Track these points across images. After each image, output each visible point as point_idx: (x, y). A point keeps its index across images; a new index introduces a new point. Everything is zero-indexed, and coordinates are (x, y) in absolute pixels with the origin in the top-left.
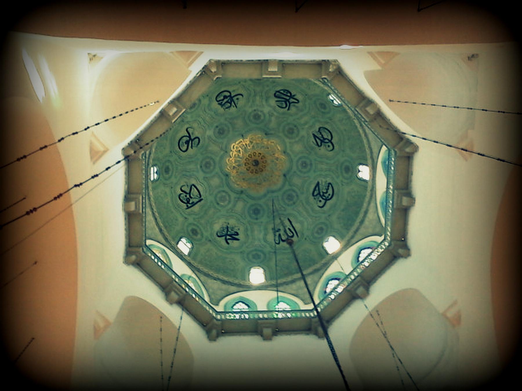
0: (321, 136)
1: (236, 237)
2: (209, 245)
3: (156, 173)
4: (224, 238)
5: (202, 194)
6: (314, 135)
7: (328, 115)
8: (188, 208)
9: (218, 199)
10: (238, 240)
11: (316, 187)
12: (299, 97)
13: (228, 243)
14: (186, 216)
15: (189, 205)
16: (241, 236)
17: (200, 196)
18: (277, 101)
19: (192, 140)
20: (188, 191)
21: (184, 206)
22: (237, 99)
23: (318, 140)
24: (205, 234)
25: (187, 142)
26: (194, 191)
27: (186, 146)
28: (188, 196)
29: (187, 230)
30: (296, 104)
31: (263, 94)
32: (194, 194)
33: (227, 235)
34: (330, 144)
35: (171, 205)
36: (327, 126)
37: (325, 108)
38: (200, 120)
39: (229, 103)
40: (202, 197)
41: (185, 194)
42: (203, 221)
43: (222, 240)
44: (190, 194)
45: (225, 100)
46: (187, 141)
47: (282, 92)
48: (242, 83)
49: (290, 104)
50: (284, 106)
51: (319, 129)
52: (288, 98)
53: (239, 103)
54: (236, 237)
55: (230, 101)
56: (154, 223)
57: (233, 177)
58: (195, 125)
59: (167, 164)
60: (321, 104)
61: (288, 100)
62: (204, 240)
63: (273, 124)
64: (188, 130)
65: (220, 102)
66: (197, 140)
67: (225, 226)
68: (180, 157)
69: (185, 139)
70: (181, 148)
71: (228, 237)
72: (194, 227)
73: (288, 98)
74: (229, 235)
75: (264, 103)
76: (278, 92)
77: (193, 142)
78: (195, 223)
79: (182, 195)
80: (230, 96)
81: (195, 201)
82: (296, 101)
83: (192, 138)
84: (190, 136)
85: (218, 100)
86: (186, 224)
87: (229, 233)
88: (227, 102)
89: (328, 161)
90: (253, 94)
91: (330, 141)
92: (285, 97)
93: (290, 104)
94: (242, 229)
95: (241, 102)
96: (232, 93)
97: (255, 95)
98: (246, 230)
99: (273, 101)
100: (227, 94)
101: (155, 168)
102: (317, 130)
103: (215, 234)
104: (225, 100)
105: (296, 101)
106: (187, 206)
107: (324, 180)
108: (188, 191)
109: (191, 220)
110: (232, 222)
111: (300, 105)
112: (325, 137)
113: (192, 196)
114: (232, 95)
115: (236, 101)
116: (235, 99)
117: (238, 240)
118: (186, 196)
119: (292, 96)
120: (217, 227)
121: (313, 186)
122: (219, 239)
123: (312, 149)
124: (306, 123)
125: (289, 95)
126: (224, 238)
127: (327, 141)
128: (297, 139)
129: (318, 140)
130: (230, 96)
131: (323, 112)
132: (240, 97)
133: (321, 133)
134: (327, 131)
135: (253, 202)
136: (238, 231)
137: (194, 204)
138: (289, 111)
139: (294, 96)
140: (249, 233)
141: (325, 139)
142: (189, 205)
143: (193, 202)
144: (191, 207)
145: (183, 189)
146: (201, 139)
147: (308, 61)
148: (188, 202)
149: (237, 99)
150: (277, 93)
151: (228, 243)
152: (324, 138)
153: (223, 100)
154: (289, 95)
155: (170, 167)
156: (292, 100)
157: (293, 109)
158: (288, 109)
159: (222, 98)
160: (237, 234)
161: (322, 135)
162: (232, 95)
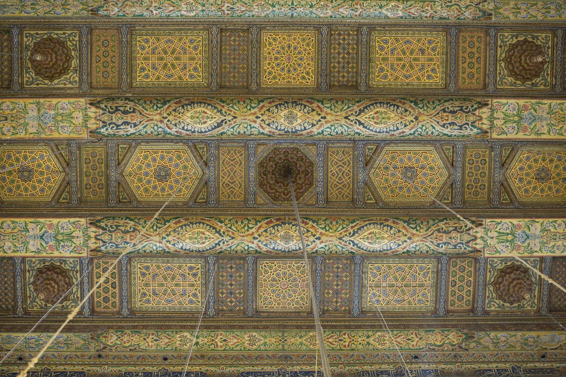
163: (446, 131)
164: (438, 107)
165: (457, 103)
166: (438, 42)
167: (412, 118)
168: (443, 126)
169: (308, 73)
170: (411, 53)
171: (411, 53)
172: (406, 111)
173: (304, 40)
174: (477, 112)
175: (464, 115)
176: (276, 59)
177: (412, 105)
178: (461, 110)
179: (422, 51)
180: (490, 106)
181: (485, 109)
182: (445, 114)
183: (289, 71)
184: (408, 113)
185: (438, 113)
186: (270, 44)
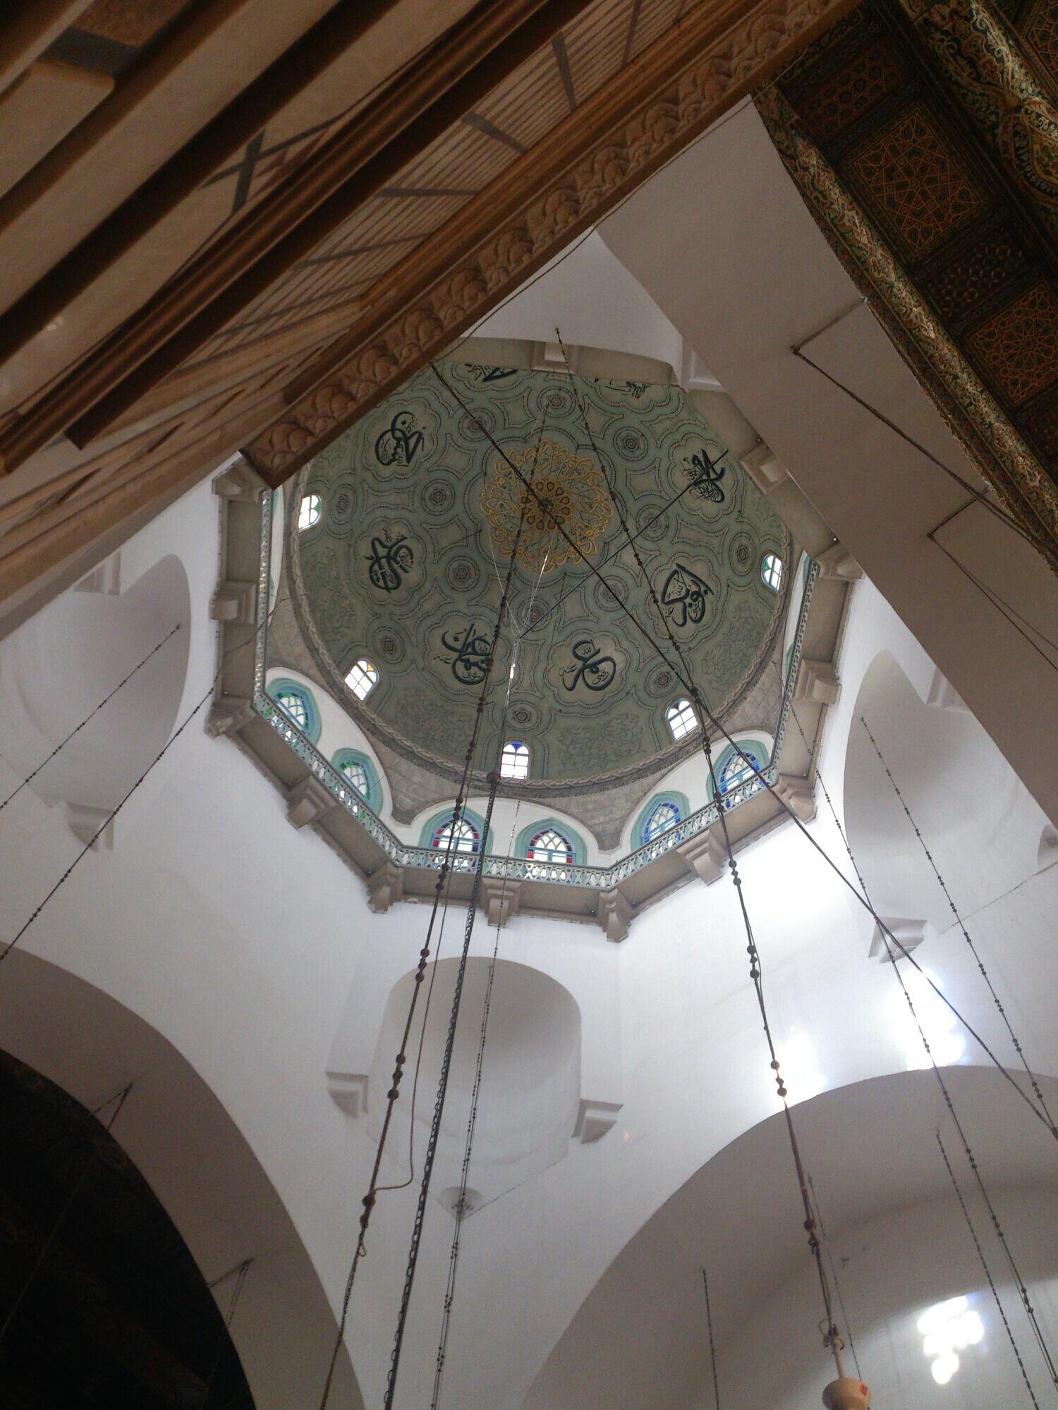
0: (399, 450)
1: (701, 459)
2: (748, 512)
3: (676, 707)
4: (717, 483)
5: (667, 574)
6: (409, 460)
7: (349, 480)
8: (708, 590)
9: (659, 532)
10: (704, 452)
11: (498, 377)
12: (365, 549)
13: (723, 470)
14: (725, 587)
15: (703, 589)
16: (694, 448)
17: (675, 572)
18: (406, 571)
19: (586, 660)
20: (679, 606)
21: (709, 598)
22: (456, 639)
23: (411, 447)
24: (735, 528)
25: (594, 668)
26: (674, 591)
27: (602, 666)
28: (688, 601)
29: (750, 570)
30: (383, 538)
31: (412, 605)
32: (677, 589)
33: (712, 481)
34: (399, 425)
35: (719, 637)
36: (374, 460)
37: (344, 498)
38: (539, 675)
39: (474, 649)
40: (675, 567)
41: (689, 609)
42: (715, 542)
43: (726, 484)
44: (681, 599)
45: (473, 658)
46: (593, 672)
47: (381, 583)
48: (421, 664)
49: (391, 547)
50: (404, 550)
51: (389, 464)
52: (384, 561)
53: (461, 630)
54: (701, 459)
55: (470, 650)
56: (754, 694)
57: (601, 528)
58: (554, 676)
59: (653, 688)
60: (341, 509)
61: (388, 557)
62: (746, 527)
63: (453, 533)
64: (569, 686)
65: (484, 666)
66: (580, 653)
67: (696, 492)
68: (629, 663)
69: (591, 678)
70: (611, 672)
71: (713, 476)
72: (735, 558)
73: (384, 561)
74: (708, 475)
75: (428, 586)
76: (387, 588)
77: (587, 656)
78: (726, 560)
79: (693, 615)
80: (460, 659)
81: (688, 579)
82: (377, 544)
83: (580, 664)
84: (582, 671)
85: (481, 674)
86: (737, 580)
87: (704, 477)
88: (475, 653)
89: (432, 398)
90: (429, 621)
91: (393, 429)
92: (387, 568)
93: (391, 547)
94: (679, 454)
95: (456, 626)
96: (452, 661)
97: (428, 615)
98: (676, 445)
99: (412, 577)
100: (460, 667)
101: (670, 716)
102: (395, 463)
103: (720, 505)
104: (473, 658)
105: (377, 544)
106: (706, 592)
107: (472, 376)
108: (679, 606)
109: (725, 572)
110: (682, 481)
111: (376, 533)
112: (393, 443)
113: (683, 593)
114: (456, 655)
115: (462, 638)
116: (459, 645)
117: (704, 452)
118: (691, 605)
119: (376, 559)
120: (710, 507)
121: (497, 382)
122: (727, 495)
123: (434, 439)
124: (399, 490)
125: (376, 567)
126: (717, 483)
127: (398, 434)
128: (443, 475)
129: (411, 447)
130: (460, 659)
131: (355, 492)
132: (450, 641)
133: (394, 455)
134: (381, 450)
135: (618, 460)
136: (690, 459)
137: (697, 580)
138: (405, 534)
139: (371, 558)
140: (678, 437)
141: (398, 440)
142: (703, 589)
143: (695, 583)
144: (705, 585)
145: (681, 622)
146: (575, 642)
147: (250, 757)
148: (698, 594)
149: (456, 639)
150: (390, 585)
151: (723, 470)
152: (398, 443)
153: (476, 664)
154: (376, 567)
155: (654, 676)
156: (382, 552)
157: (397, 531)
158: (404, 538)
159: (474, 669)
160: (695, 458)
161: (395, 449)
162: (456, 655)
163: (1005, 49)
164: (979, 90)
165: (951, 67)
166: (862, 161)
167: (1022, 115)
168: (1001, 60)
169: (1032, 304)
170: (904, 185)
171: (904, 185)
172: (1016, 133)
173: (989, 346)
174: (948, 27)
175: (964, 43)
176: (1040, 361)
177: (999, 131)
178: (959, 53)
179: (890, 173)
180: (926, 15)
181: (937, 18)
182: (984, 72)
183: (1046, 332)
184: (1019, 128)
185: (989, 83)
186: (1024, 385)
